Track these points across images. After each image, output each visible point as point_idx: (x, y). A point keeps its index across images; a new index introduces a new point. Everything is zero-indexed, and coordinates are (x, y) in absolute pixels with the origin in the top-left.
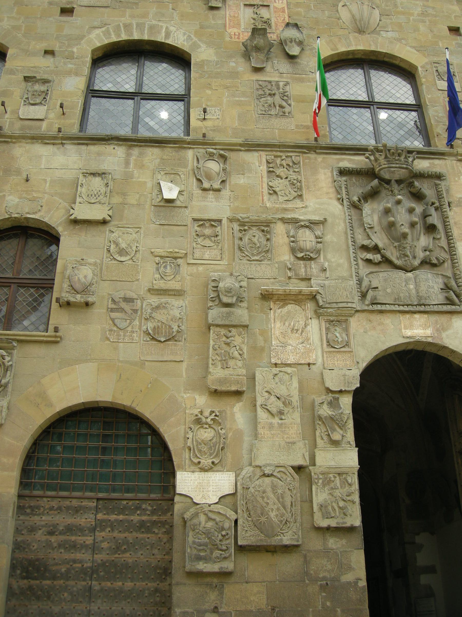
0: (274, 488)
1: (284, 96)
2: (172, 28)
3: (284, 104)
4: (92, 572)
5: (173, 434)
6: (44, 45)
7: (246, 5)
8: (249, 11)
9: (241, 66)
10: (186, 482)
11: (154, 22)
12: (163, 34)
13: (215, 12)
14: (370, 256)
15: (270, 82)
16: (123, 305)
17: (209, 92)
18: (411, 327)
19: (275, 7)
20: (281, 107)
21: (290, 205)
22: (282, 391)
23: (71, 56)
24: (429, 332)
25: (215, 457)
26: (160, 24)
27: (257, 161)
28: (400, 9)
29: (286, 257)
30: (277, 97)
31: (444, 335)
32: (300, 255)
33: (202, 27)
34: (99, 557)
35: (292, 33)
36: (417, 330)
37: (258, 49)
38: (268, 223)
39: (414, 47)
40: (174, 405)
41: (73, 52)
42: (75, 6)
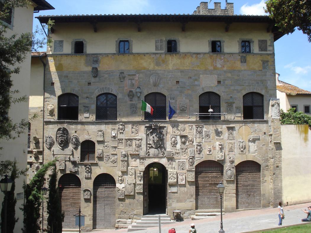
0: (130, 186)
1: (136, 108)
2: (113, 89)
3: (136, 110)
4: (104, 198)
5: (116, 178)
6: (85, 95)
7: (129, 79)
8: (130, 81)
9: (127, 99)
10: (118, 185)
11: (109, 87)
12: (111, 90)
13: (122, 82)
14: (149, 146)
15: (133, 104)
16: (107, 156)
17: (121, 107)
18: (155, 160)
19: (136, 80)
20: (135, 111)
21: (136, 135)
22: (132, 171)
23: (92, 98)
24: (158, 161)
25: (122, 181)
26: (110, 87)
27: (130, 126)
28: (165, 76)
29: (135, 146)
30: (134, 108)
31: (160, 161)
32: (137, 146)
33: (119, 87)
34: (106, 195)
35: (138, 90)
36: (156, 160)
37: (131, 95)
38: (131, 139)
39: (166, 90)
40: (116, 174)
41: (92, 97)
42: (91, 82)
